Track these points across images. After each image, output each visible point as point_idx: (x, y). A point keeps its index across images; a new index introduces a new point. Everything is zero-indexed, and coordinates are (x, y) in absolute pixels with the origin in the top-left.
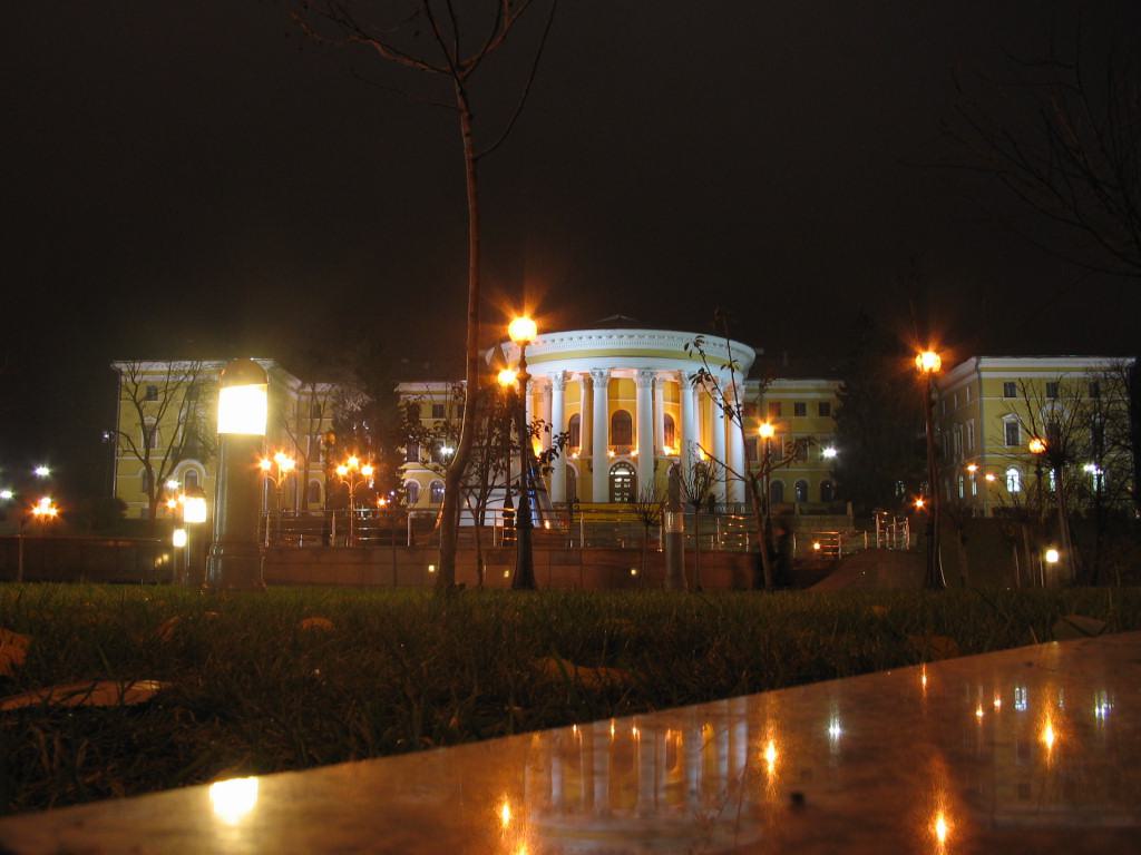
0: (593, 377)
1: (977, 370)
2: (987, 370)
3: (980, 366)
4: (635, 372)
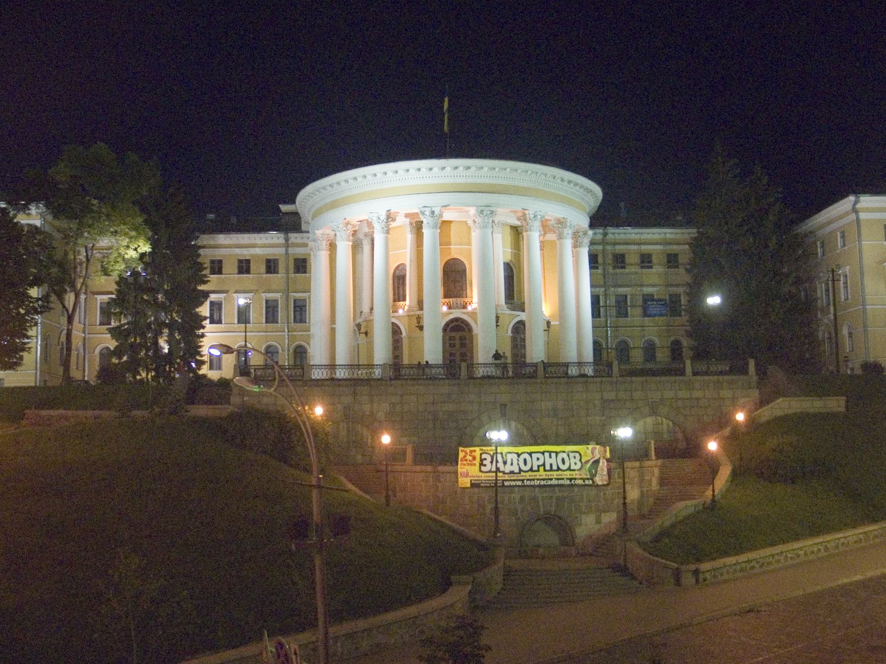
0: (422, 218)
1: (855, 210)
2: (868, 210)
3: (858, 206)
4: (472, 211)
